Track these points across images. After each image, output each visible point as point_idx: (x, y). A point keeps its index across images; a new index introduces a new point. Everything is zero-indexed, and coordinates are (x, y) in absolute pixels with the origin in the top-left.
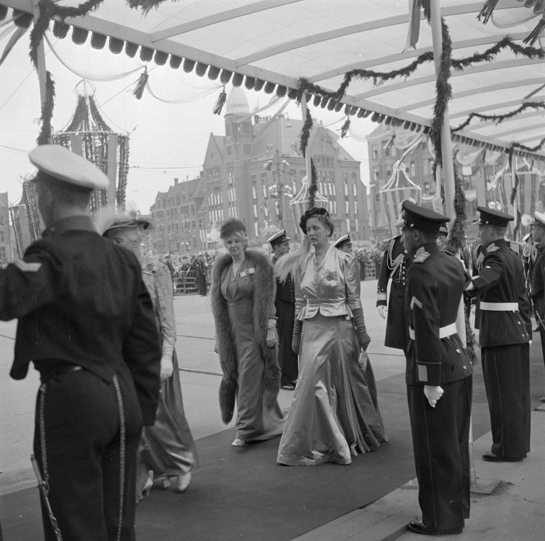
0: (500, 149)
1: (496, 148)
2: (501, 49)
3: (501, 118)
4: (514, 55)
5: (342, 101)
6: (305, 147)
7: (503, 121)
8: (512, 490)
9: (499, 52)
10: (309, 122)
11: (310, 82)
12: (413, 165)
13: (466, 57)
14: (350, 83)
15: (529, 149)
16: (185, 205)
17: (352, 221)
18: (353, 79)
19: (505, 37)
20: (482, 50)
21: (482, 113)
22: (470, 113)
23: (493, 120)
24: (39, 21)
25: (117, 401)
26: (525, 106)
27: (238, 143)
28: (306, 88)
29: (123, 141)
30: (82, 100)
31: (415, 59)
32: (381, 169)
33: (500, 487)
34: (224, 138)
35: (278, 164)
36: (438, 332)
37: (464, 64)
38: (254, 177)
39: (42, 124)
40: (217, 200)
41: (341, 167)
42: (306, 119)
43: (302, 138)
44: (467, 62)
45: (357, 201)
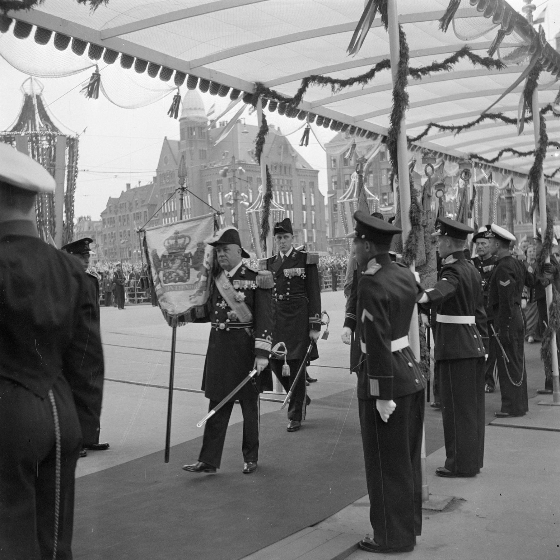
1: (452, 159)
2: (460, 58)
3: (460, 128)
4: (472, 64)
5: (301, 107)
7: (461, 131)
8: (465, 507)
9: (458, 61)
10: (264, 128)
11: (266, 86)
12: (372, 175)
13: (425, 65)
14: (307, 89)
15: (487, 161)
16: (137, 211)
17: (309, 232)
18: (310, 85)
19: (463, 46)
20: (440, 59)
21: (441, 124)
22: (429, 123)
25: (53, 416)
26: (484, 116)
27: (193, 148)
28: (261, 93)
29: (72, 143)
30: (28, 99)
31: (373, 66)
32: (339, 178)
33: (453, 503)
34: (179, 143)
35: (234, 171)
36: (390, 345)
38: (209, 183)
40: (171, 207)
41: (299, 175)
42: (261, 124)
43: (257, 144)
44: (425, 71)
45: (315, 211)
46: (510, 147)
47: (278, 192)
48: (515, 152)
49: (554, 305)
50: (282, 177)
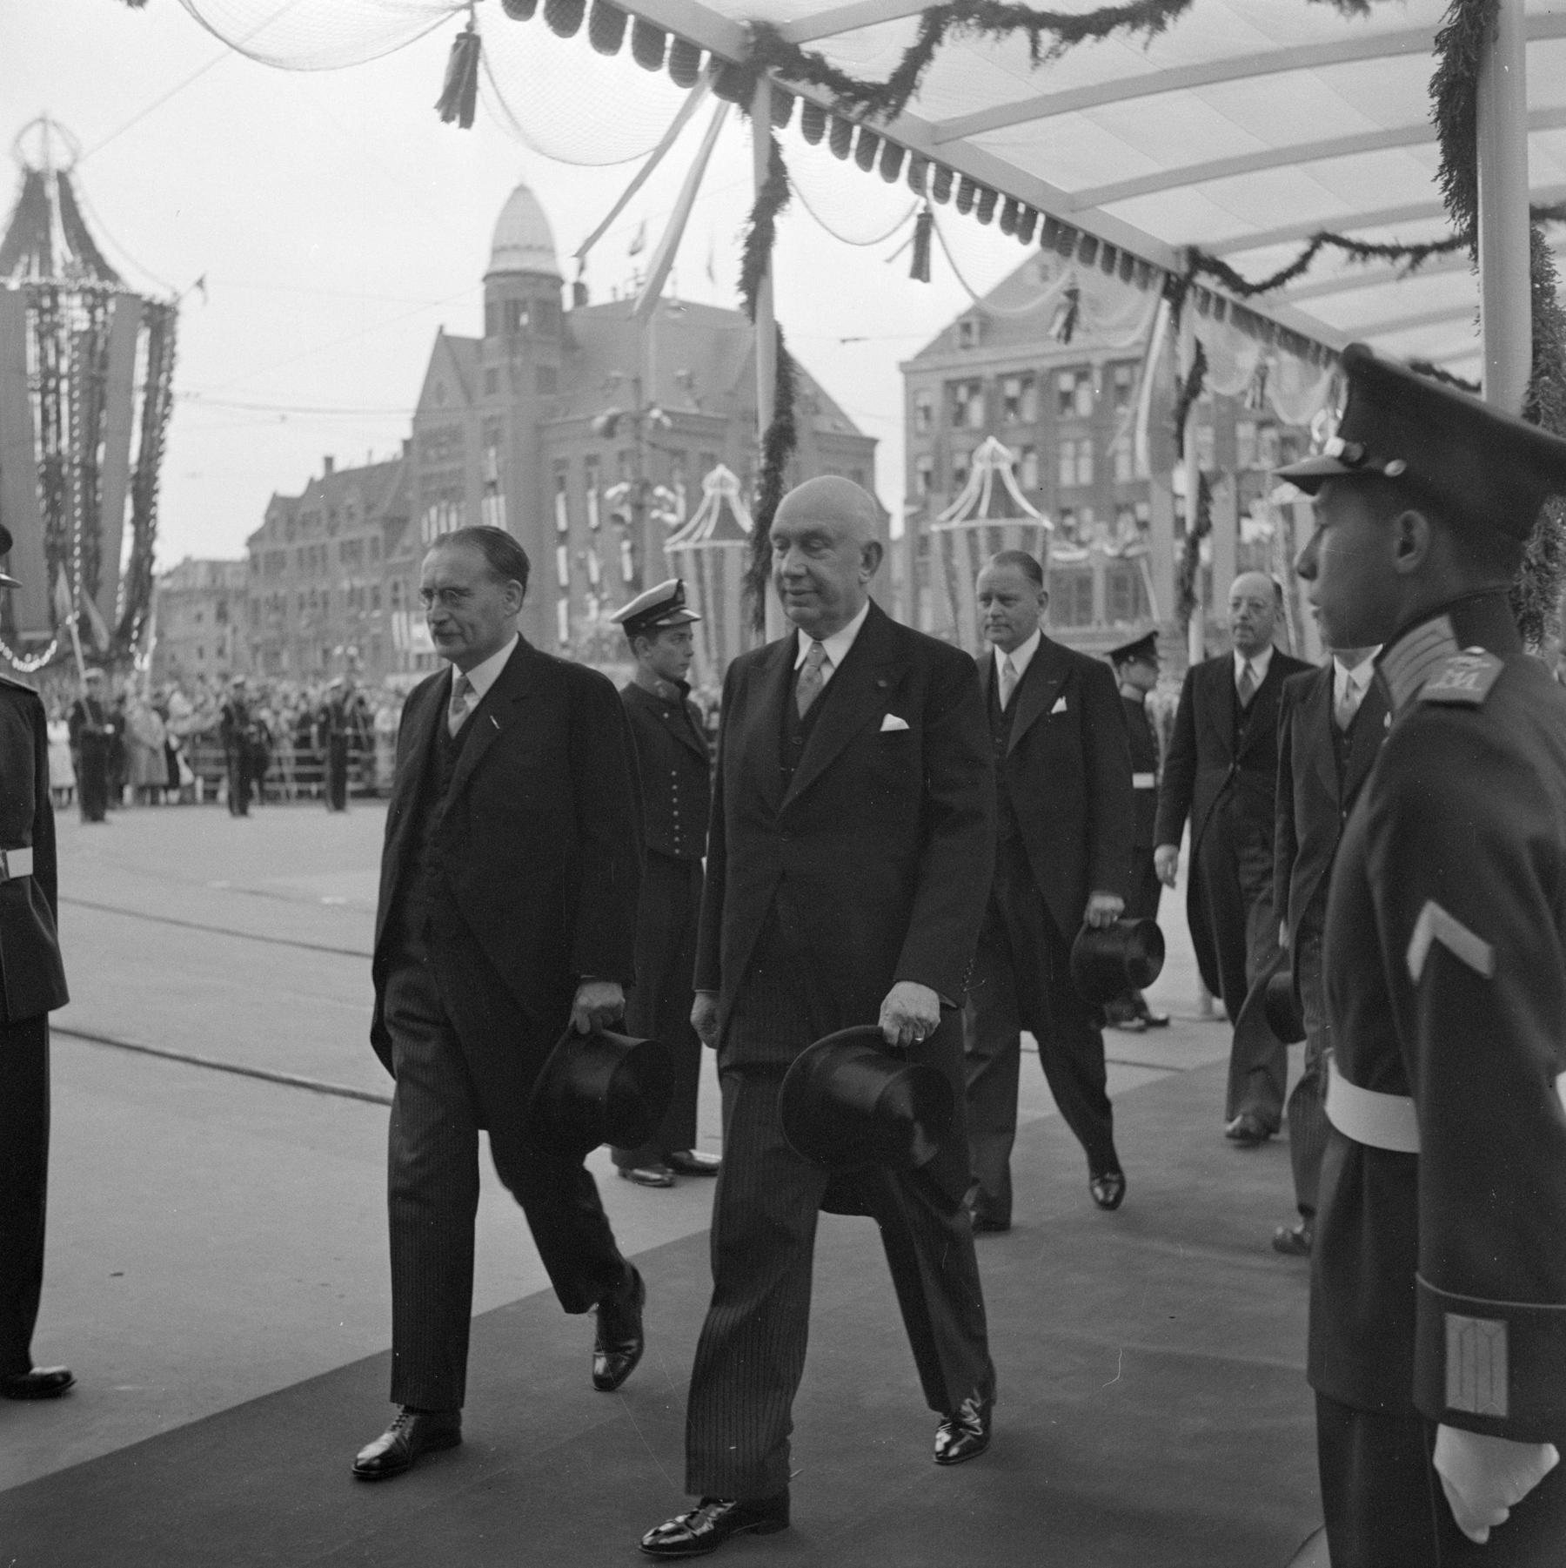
3: (1419, 252)
6: (757, 281)
11: (790, 38)
12: (1032, 457)
14: (936, 49)
16: (352, 535)
21: (1354, 236)
22: (1314, 231)
23: (1389, 258)
27: (518, 361)
28: (768, 62)
29: (160, 319)
30: (33, 183)
32: (938, 464)
34: (478, 344)
35: (638, 420)
38: (562, 464)
42: (766, 175)
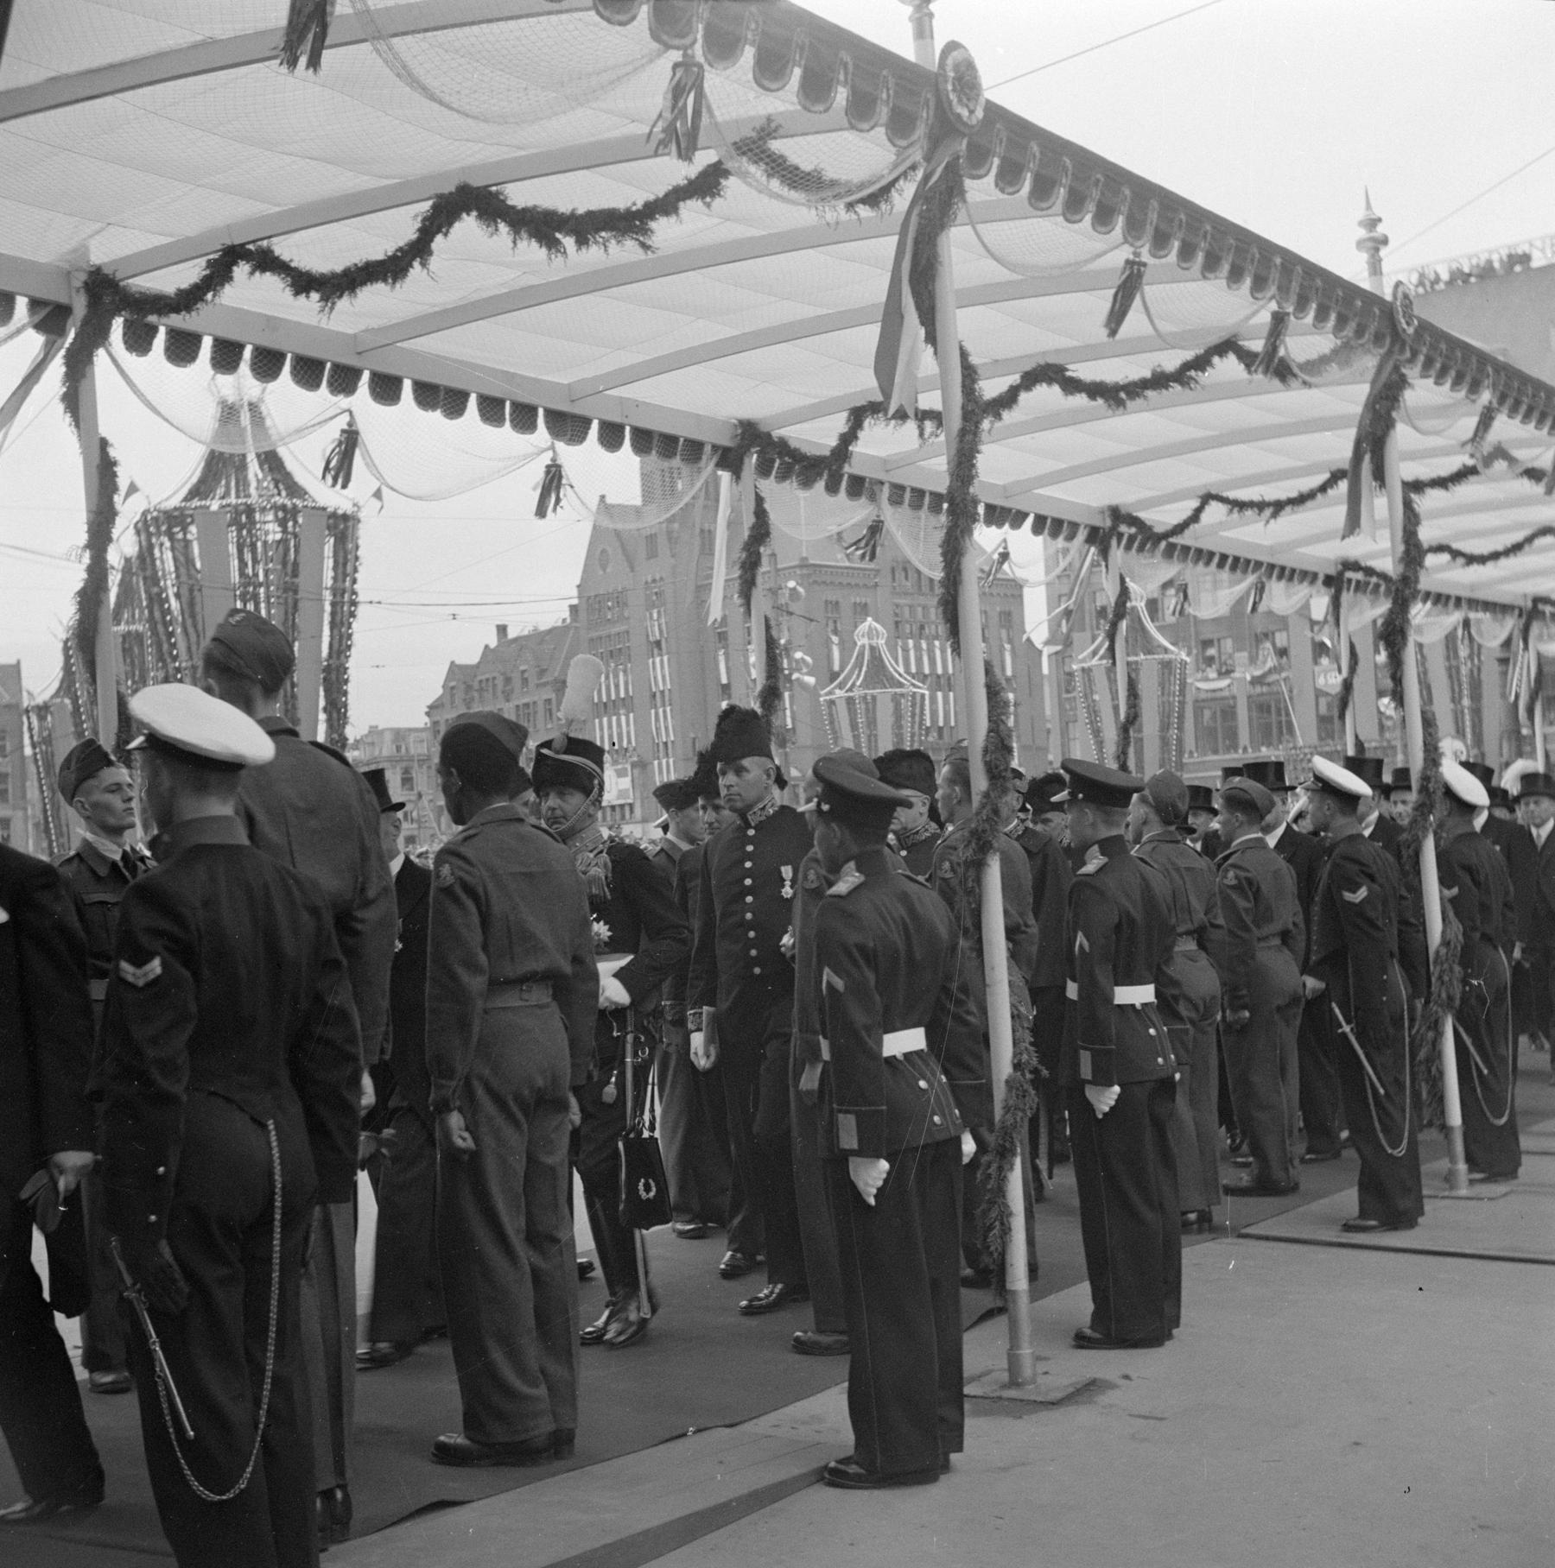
0: (1309, 579)
1: (1287, 574)
2: (1216, 360)
3: (1278, 507)
11: (763, 428)
14: (861, 434)
16: (525, 701)
20: (1171, 361)
21: (1232, 494)
22: (1202, 492)
24: (86, 322)
31: (1015, 379)
33: (1088, 1390)
37: (1128, 394)
39: (87, 559)
40: (617, 686)
43: (743, 567)
44: (1135, 389)
46: (1444, 542)
47: (911, 642)
48: (1456, 554)
49: (1443, 951)
50: (922, 600)
